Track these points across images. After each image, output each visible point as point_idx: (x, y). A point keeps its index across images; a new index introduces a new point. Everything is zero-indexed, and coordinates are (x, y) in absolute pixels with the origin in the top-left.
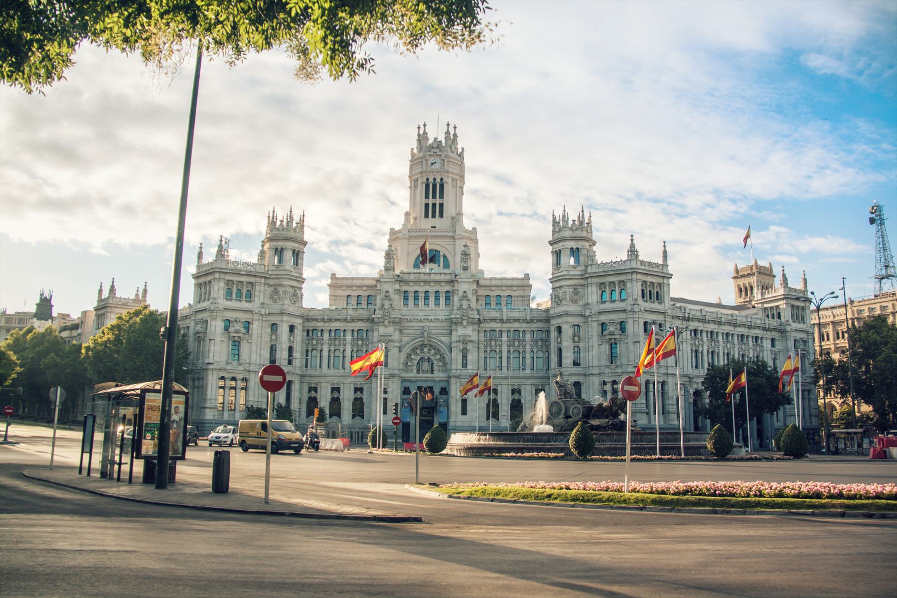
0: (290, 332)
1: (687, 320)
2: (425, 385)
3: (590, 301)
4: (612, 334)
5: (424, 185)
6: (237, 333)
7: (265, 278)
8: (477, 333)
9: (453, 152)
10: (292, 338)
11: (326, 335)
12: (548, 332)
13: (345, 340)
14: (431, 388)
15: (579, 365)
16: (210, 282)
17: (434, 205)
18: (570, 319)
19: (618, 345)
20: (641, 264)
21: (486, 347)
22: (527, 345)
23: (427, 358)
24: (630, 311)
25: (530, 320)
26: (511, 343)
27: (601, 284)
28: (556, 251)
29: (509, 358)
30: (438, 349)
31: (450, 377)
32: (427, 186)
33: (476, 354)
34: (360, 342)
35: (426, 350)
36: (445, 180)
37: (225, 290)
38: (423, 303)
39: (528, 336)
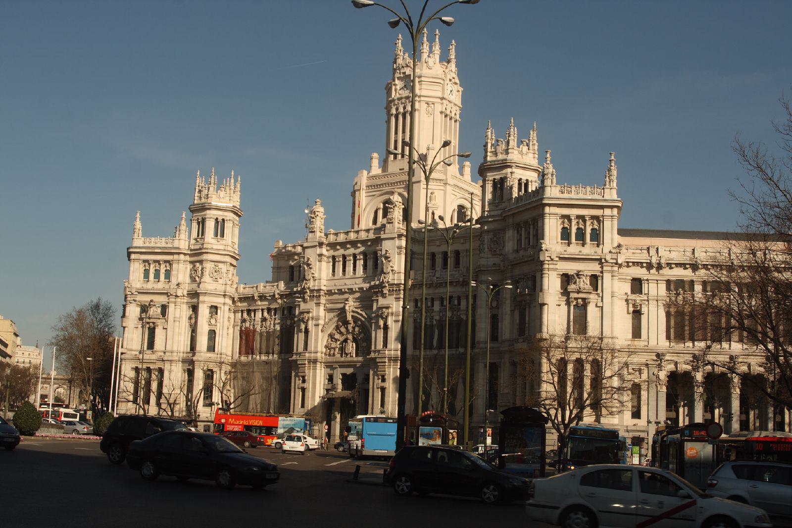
2: (349, 371)
5: (393, 120)
7: (185, 254)
11: (259, 315)
23: (350, 337)
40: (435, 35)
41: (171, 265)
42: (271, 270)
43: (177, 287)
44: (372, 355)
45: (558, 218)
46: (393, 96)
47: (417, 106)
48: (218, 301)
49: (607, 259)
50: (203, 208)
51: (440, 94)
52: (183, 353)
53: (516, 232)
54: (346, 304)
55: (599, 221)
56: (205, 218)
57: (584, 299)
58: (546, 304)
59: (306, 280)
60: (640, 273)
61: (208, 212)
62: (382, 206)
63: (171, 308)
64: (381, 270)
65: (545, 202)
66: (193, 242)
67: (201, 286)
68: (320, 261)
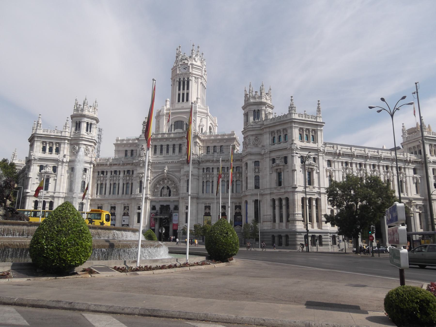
1: (338, 155)
2: (165, 204)
3: (265, 144)
4: (278, 165)
5: (178, 83)
8: (197, 170)
9: (197, 62)
11: (109, 174)
13: (119, 177)
14: (168, 207)
15: (259, 188)
17: (183, 94)
18: (253, 157)
20: (299, 116)
21: (203, 178)
23: (166, 186)
24: (289, 149)
30: (173, 181)
31: (179, 198)
32: (180, 83)
34: (128, 178)
35: (166, 181)
36: (189, 79)
37: (42, 147)
38: (166, 152)
41: (60, 144)
42: (114, 151)
44: (181, 195)
45: (298, 129)
46: (178, 73)
47: (191, 78)
48: (87, 166)
51: (200, 74)
53: (270, 135)
54: (165, 169)
55: (315, 132)
57: (312, 168)
58: (296, 170)
60: (330, 158)
62: (173, 123)
63: (59, 169)
66: (72, 133)
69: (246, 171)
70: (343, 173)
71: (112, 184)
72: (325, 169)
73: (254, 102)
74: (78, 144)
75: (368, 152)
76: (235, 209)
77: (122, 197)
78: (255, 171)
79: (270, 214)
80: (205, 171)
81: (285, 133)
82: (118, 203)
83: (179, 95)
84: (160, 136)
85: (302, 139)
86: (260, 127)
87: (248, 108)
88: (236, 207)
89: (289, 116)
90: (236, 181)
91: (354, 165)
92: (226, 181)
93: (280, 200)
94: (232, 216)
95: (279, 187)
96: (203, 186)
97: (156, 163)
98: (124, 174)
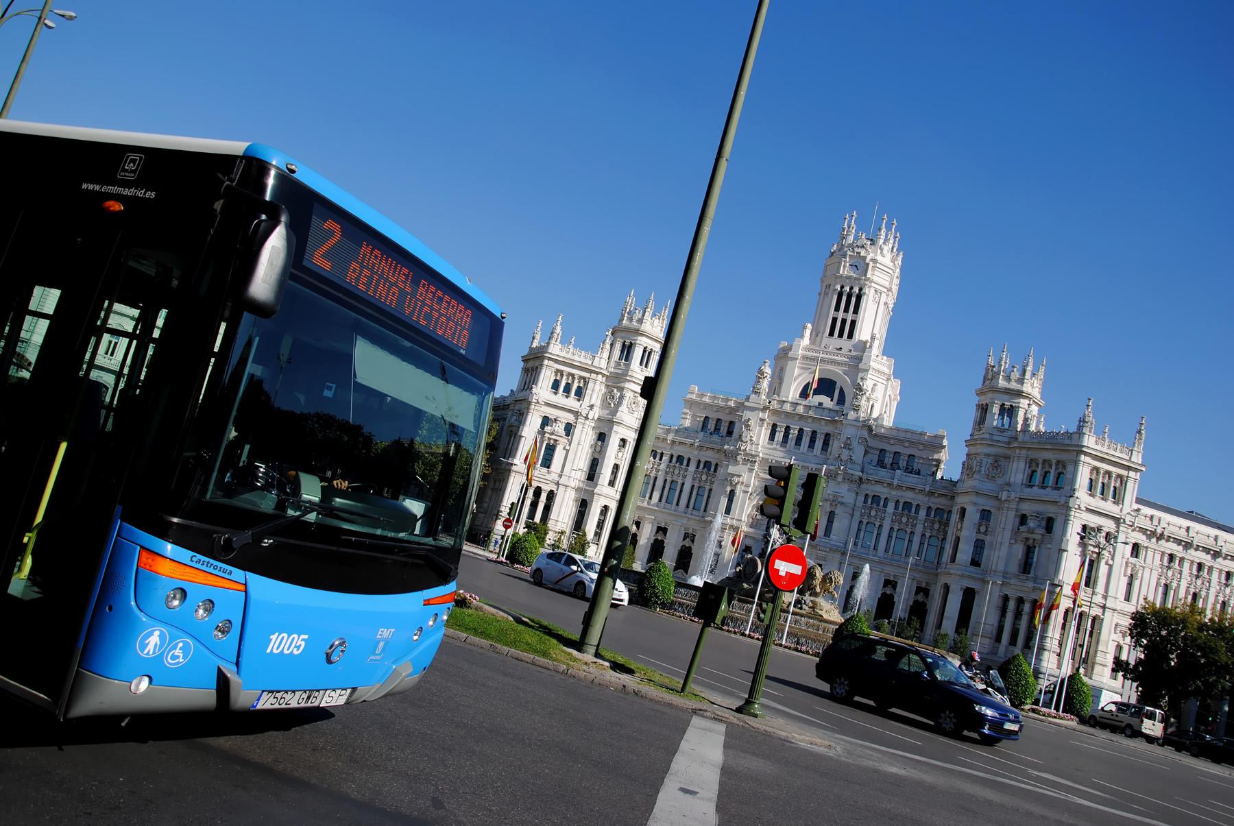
0: (619, 446)
6: (552, 434)
10: (620, 455)
12: (950, 512)
13: (686, 470)
16: (537, 368)
17: (844, 321)
18: (981, 500)
19: (1037, 549)
20: (1096, 442)
21: (862, 515)
22: (918, 525)
24: (1063, 505)
25: (929, 492)
26: (897, 519)
27: (1032, 460)
28: (982, 405)
29: (890, 537)
32: (840, 295)
33: (846, 522)
34: (704, 477)
36: (863, 291)
37: (552, 381)
39: (922, 513)
40: (893, 224)
43: (589, 408)
46: (841, 273)
47: (866, 290)
49: (1126, 520)
50: (637, 332)
51: (887, 285)
52: (579, 481)
53: (1028, 465)
56: (635, 344)
59: (742, 441)
61: (640, 338)
64: (837, 456)
65: (1084, 449)
66: (612, 364)
67: (618, 414)
68: (761, 426)
69: (960, 524)
70: (1160, 576)
71: (668, 481)
72: (1125, 560)
73: (1006, 389)
74: (621, 389)
75: (1223, 544)
76: (916, 594)
77: (685, 513)
78: (979, 529)
79: (991, 623)
80: (870, 501)
81: (1060, 470)
82: (673, 522)
83: (835, 320)
84: (787, 408)
85: (1092, 490)
86: (1009, 442)
87: (990, 395)
88: (919, 590)
89: (1075, 437)
90: (930, 537)
91: (1186, 565)
92: (908, 532)
93: (1020, 601)
94: (907, 606)
95: (1023, 576)
96: (859, 530)
97: (770, 461)
98: (698, 467)
